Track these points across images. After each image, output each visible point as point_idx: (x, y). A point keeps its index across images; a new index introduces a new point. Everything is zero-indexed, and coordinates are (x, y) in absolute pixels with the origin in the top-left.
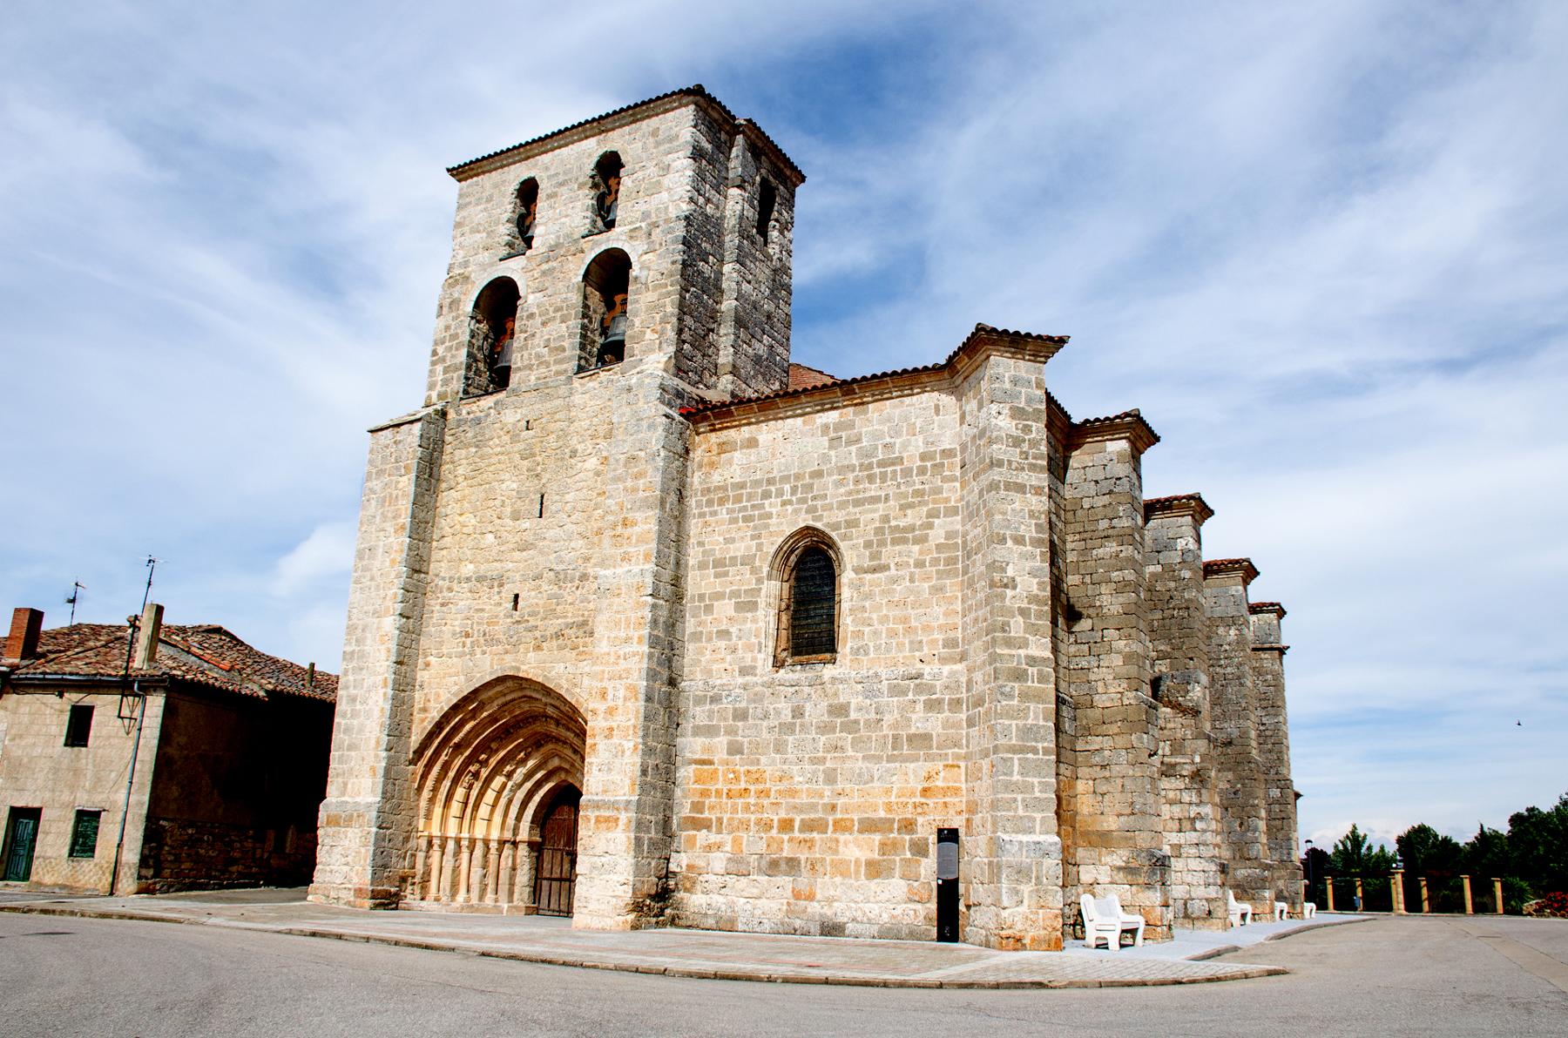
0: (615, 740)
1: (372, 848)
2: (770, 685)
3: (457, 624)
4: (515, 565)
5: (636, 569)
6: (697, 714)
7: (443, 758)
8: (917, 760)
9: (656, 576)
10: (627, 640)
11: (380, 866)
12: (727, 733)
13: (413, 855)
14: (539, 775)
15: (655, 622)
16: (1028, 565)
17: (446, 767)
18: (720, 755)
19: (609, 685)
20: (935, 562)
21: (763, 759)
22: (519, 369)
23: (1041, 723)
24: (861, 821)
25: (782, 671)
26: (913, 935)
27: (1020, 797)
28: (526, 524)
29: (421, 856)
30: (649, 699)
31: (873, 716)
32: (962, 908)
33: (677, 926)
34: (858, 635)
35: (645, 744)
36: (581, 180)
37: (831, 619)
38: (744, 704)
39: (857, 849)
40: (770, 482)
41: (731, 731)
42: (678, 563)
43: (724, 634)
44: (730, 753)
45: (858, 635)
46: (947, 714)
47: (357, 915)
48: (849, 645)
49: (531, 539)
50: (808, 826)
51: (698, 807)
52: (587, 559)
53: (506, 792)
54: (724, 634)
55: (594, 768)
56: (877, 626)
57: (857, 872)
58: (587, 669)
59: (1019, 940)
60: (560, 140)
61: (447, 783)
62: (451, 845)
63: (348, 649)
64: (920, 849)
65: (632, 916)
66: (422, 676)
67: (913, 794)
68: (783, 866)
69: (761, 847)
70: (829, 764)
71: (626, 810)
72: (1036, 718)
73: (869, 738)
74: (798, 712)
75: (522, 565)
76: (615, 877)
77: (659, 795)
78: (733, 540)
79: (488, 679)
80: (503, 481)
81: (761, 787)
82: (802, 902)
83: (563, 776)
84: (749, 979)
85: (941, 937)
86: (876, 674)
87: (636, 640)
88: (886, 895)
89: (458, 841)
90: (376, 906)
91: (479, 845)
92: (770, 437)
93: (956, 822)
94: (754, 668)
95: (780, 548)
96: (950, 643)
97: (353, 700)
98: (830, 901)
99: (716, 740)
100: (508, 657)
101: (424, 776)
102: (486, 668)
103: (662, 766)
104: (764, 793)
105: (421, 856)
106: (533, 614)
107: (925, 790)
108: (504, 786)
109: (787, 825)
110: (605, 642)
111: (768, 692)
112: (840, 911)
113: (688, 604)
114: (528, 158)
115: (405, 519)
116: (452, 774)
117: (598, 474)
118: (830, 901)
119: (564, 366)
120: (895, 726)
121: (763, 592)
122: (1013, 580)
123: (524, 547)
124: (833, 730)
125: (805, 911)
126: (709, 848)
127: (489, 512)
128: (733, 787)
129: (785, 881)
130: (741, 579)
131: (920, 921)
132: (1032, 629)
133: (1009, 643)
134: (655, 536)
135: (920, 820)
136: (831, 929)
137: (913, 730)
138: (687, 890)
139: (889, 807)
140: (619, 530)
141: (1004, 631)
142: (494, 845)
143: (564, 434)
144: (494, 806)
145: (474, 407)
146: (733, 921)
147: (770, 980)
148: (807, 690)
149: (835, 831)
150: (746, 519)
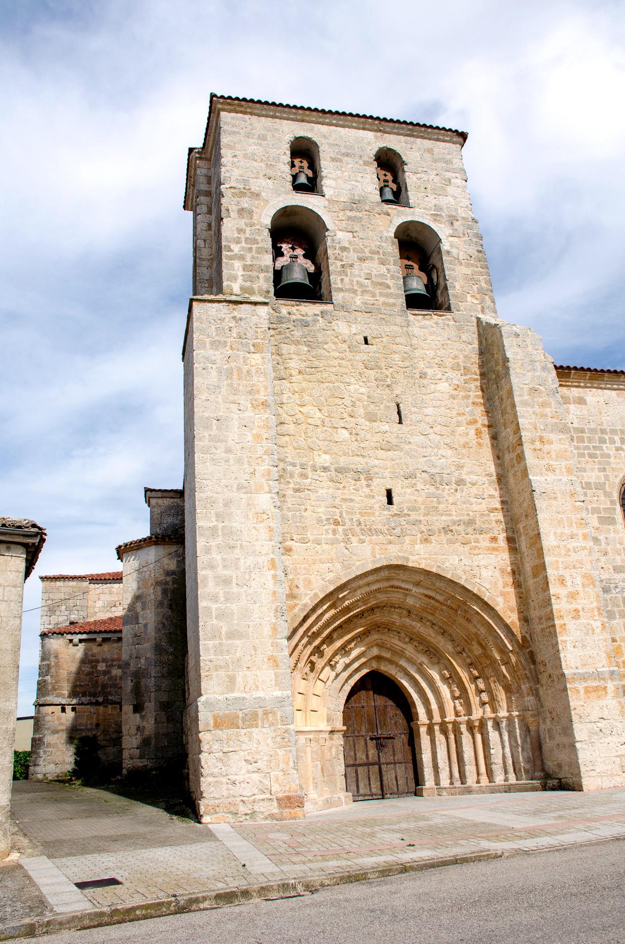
0: (583, 621)
4: (380, 461)
14: (356, 665)
19: (567, 574)
22: (341, 290)
28: (386, 427)
36: (366, 159)
40: (603, 431)
49: (394, 441)
52: (460, 467)
55: (568, 645)
58: (482, 563)
60: (341, 120)
71: (612, 679)
78: (585, 470)
79: (370, 567)
80: (349, 384)
83: (374, 665)
92: (595, 399)
102: (367, 556)
110: (552, 537)
114: (303, 121)
117: (453, 397)
119: (391, 301)
123: (388, 447)
140: (538, 445)
143: (407, 357)
145: (294, 309)
150: (591, 456)
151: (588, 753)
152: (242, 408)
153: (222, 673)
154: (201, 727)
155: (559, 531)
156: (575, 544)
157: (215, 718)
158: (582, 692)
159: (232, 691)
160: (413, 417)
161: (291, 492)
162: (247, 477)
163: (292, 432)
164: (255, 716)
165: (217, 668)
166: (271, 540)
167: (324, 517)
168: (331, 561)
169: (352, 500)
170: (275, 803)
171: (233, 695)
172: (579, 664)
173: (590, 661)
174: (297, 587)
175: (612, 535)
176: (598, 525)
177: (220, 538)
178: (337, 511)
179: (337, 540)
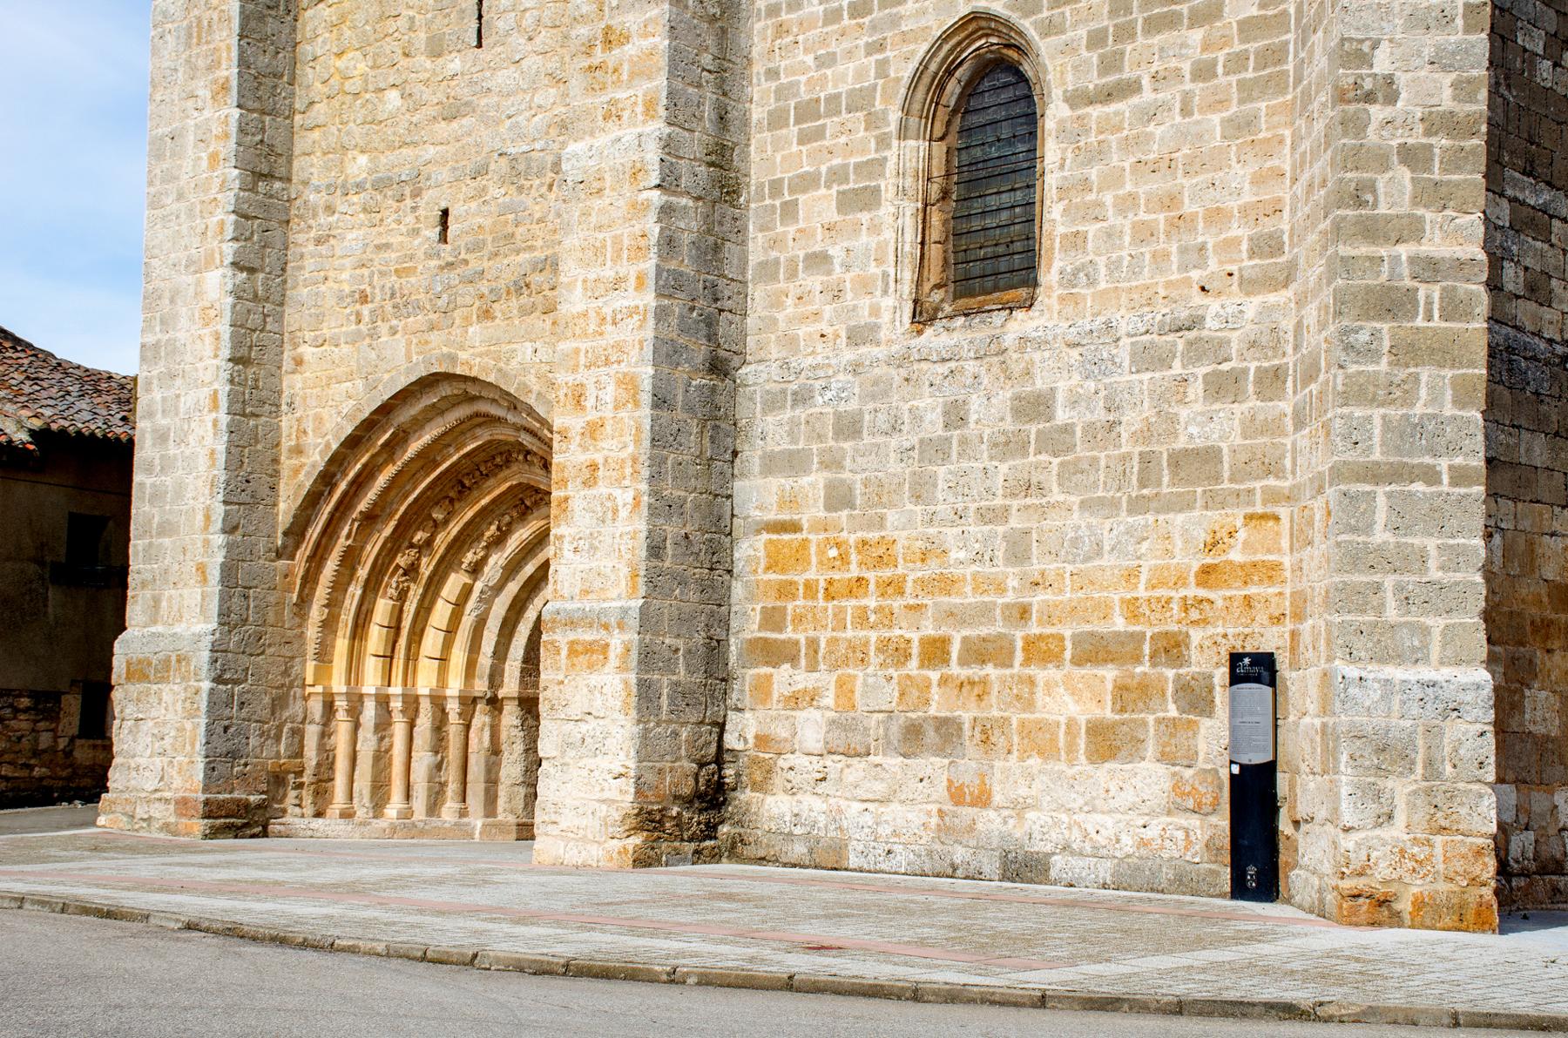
0: (602, 489)
1: (203, 721)
2: (903, 360)
3: (346, 279)
5: (629, 135)
6: (767, 430)
7: (342, 543)
8: (1186, 505)
9: (668, 145)
10: (617, 284)
11: (223, 754)
12: (825, 465)
13: (298, 733)
15: (669, 243)
16: (1430, 43)
17: (350, 559)
18: (812, 512)
19: (586, 377)
20: (1237, 62)
21: (892, 516)
23: (1449, 411)
24: (1078, 640)
25: (929, 331)
26: (1184, 883)
27: (1389, 581)
28: (454, 64)
29: (312, 732)
30: (660, 401)
31: (1100, 415)
32: (1285, 826)
33: (742, 859)
34: (1076, 241)
35: (655, 493)
37: (1028, 215)
38: (853, 405)
39: (1070, 698)
41: (832, 462)
42: (722, 119)
43: (819, 261)
44: (829, 507)
45: (1076, 241)
46: (1253, 403)
47: (185, 849)
48: (1057, 265)
49: (464, 93)
50: (978, 652)
51: (772, 618)
53: (471, 604)
54: (819, 261)
56: (1114, 220)
57: (1071, 748)
59: (1383, 902)
61: (355, 591)
62: (369, 712)
63: (150, 339)
64: (1195, 698)
65: (637, 840)
66: (293, 384)
67: (1181, 581)
68: (931, 736)
69: (888, 696)
70: (1015, 522)
71: (621, 626)
72: (1435, 399)
73: (1094, 462)
74: (955, 416)
75: (451, 149)
76: (603, 763)
77: (693, 596)
79: (402, 382)
81: (887, 573)
82: (967, 812)
84: (633, 975)
85: (1239, 890)
86: (1108, 326)
87: (632, 280)
88: (1129, 797)
89: (383, 701)
90: (214, 833)
91: (425, 707)
93: (1268, 640)
94: (875, 328)
95: (924, 66)
96: (1267, 245)
97: (162, 437)
98: (1020, 808)
99: (805, 481)
100: (434, 337)
101: (310, 579)
103: (696, 537)
104: (893, 586)
105: (312, 732)
106: (476, 247)
107: (1206, 573)
108: (467, 591)
109: (936, 651)
111: (897, 375)
112: (1039, 829)
113: (755, 204)
115: (229, 70)
116: (363, 573)
118: (1020, 808)
120: (1146, 433)
121: (891, 166)
122: (1389, 80)
124: (1023, 449)
125: (971, 829)
126: (795, 701)
127: (389, 46)
128: (837, 576)
129: (931, 764)
130: (848, 140)
131: (1197, 853)
132: (1435, 195)
133: (1371, 230)
134: (663, 62)
135: (1196, 635)
136: (1023, 867)
137: (1181, 443)
138: (757, 787)
139: (1132, 609)
140: (599, 55)
141: (1359, 202)
142: (453, 707)
144: (451, 631)
146: (839, 848)
147: (674, 979)
148: (971, 367)
149: (1027, 662)
151: (553, 785)
152: (200, 104)
153: (148, 593)
154: (114, 679)
155: (592, 276)
156: (617, 305)
157: (129, 664)
158: (564, 653)
159: (154, 622)
160: (500, 24)
161: (311, 247)
162: (196, 241)
163: (321, 120)
164: (168, 660)
165: (144, 584)
166: (216, 356)
167: (347, 289)
168: (350, 378)
169: (387, 246)
170: (172, 807)
171: (153, 629)
172: (577, 591)
173: (597, 584)
174: (305, 432)
175: (864, 238)
176: (836, 217)
177: (162, 363)
178: (366, 272)
179: (359, 331)
